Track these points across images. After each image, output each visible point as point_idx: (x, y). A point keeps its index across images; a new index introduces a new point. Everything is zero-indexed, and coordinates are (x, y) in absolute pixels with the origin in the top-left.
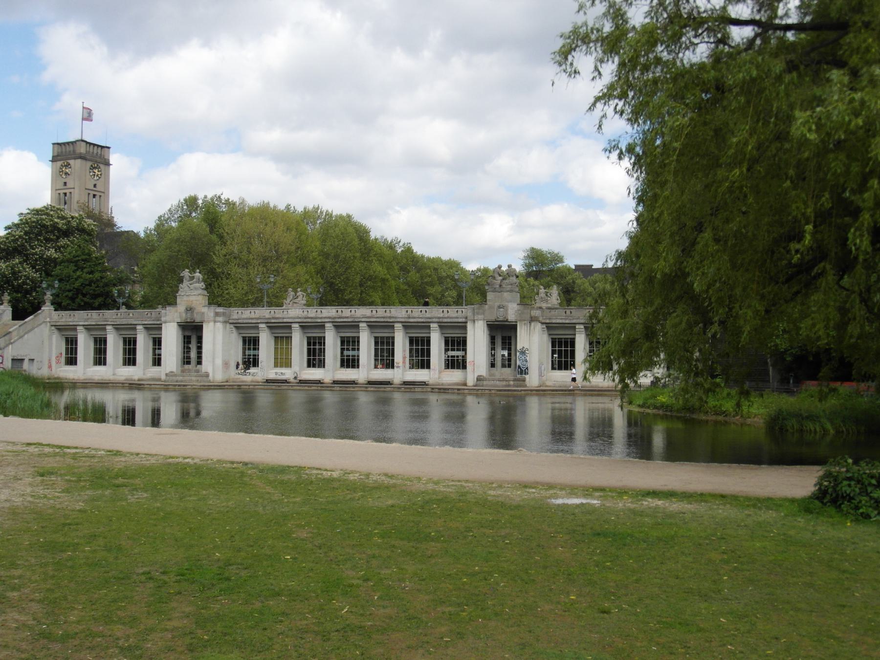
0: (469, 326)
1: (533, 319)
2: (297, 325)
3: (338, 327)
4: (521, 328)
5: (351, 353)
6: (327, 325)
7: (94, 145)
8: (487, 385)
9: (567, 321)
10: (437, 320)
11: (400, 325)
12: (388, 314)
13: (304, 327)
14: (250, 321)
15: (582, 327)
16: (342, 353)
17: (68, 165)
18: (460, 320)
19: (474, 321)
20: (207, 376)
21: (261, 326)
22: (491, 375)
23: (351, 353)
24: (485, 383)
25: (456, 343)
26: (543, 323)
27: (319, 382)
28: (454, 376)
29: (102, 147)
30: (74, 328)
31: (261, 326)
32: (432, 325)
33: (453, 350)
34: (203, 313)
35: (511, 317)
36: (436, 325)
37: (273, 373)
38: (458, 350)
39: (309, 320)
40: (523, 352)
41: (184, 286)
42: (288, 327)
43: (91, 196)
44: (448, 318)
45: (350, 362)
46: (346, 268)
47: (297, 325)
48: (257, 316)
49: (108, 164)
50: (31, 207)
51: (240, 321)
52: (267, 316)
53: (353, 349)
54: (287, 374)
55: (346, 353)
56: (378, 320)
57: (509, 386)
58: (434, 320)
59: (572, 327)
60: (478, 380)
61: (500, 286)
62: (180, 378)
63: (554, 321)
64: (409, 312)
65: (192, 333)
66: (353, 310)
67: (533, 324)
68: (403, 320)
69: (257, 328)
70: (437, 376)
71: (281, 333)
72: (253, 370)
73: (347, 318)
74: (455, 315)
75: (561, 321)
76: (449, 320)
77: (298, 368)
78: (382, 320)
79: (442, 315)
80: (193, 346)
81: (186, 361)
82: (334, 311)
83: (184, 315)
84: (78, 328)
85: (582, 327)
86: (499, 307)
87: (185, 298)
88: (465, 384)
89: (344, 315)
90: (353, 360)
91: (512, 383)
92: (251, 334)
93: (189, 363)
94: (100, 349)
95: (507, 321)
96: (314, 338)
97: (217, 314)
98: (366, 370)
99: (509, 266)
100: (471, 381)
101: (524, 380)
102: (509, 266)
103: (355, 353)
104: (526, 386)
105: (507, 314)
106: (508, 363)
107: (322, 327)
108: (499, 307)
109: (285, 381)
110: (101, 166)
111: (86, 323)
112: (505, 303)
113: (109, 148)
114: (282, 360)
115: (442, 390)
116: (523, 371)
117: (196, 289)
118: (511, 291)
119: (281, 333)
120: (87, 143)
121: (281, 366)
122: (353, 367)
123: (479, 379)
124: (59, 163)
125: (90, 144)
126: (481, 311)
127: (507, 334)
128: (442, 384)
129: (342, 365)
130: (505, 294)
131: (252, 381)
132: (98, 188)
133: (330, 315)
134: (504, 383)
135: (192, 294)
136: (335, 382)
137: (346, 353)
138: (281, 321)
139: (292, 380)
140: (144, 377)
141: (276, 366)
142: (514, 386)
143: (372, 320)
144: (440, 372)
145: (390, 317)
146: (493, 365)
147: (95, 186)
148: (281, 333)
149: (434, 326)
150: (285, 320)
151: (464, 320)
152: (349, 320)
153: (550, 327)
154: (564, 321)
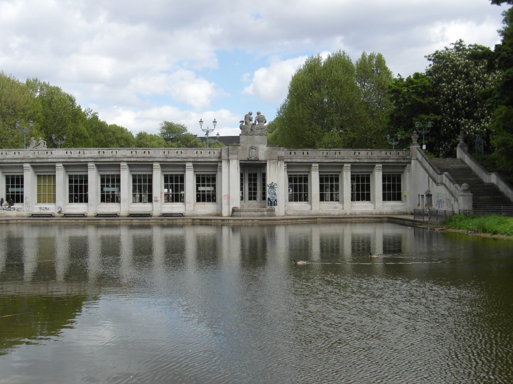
0: (224, 165)
1: (280, 159)
2: (61, 165)
6: (89, 164)
8: (244, 216)
9: (305, 161)
10: (192, 160)
11: (158, 164)
12: (147, 155)
14: (15, 161)
18: (213, 160)
19: (229, 161)
21: (25, 165)
22: (242, 206)
24: (242, 213)
25: (208, 180)
27: (83, 215)
28: (206, 209)
31: (25, 165)
33: (204, 186)
35: (262, 157)
36: (191, 164)
37: (37, 208)
38: (208, 186)
39: (73, 160)
40: (272, 187)
42: (52, 167)
44: (202, 158)
45: (114, 198)
47: (61, 165)
51: (4, 161)
52: (32, 156)
54: (51, 208)
56: (138, 160)
57: (263, 216)
60: (233, 211)
61: (252, 130)
63: (294, 161)
64: (166, 153)
66: (114, 152)
67: (279, 163)
69: (22, 167)
70: (192, 208)
72: (16, 206)
73: (109, 158)
74: (208, 155)
76: (203, 160)
77: (63, 204)
78: (142, 160)
79: (196, 156)
82: (96, 152)
86: (252, 148)
88: (220, 215)
89: (106, 155)
91: (266, 213)
92: (15, 172)
95: (258, 160)
96: (76, 176)
98: (127, 204)
99: (258, 114)
100: (226, 212)
101: (273, 210)
104: (275, 216)
105: (258, 154)
106: (252, 197)
107: (85, 166)
108: (252, 148)
109: (51, 216)
114: (47, 195)
115: (204, 222)
116: (273, 203)
118: (261, 135)
119: (43, 172)
121: (44, 202)
126: (235, 152)
127: (253, 172)
128: (197, 216)
130: (256, 137)
131: (17, 216)
134: (259, 213)
136: (98, 215)
137: (106, 189)
138: (45, 160)
139: (57, 214)
141: (39, 201)
142: (268, 216)
143: (133, 160)
145: (149, 158)
146: (242, 198)
148: (45, 172)
149: (189, 165)
150: (49, 160)
151: (216, 160)
152: (111, 160)
153: (289, 166)
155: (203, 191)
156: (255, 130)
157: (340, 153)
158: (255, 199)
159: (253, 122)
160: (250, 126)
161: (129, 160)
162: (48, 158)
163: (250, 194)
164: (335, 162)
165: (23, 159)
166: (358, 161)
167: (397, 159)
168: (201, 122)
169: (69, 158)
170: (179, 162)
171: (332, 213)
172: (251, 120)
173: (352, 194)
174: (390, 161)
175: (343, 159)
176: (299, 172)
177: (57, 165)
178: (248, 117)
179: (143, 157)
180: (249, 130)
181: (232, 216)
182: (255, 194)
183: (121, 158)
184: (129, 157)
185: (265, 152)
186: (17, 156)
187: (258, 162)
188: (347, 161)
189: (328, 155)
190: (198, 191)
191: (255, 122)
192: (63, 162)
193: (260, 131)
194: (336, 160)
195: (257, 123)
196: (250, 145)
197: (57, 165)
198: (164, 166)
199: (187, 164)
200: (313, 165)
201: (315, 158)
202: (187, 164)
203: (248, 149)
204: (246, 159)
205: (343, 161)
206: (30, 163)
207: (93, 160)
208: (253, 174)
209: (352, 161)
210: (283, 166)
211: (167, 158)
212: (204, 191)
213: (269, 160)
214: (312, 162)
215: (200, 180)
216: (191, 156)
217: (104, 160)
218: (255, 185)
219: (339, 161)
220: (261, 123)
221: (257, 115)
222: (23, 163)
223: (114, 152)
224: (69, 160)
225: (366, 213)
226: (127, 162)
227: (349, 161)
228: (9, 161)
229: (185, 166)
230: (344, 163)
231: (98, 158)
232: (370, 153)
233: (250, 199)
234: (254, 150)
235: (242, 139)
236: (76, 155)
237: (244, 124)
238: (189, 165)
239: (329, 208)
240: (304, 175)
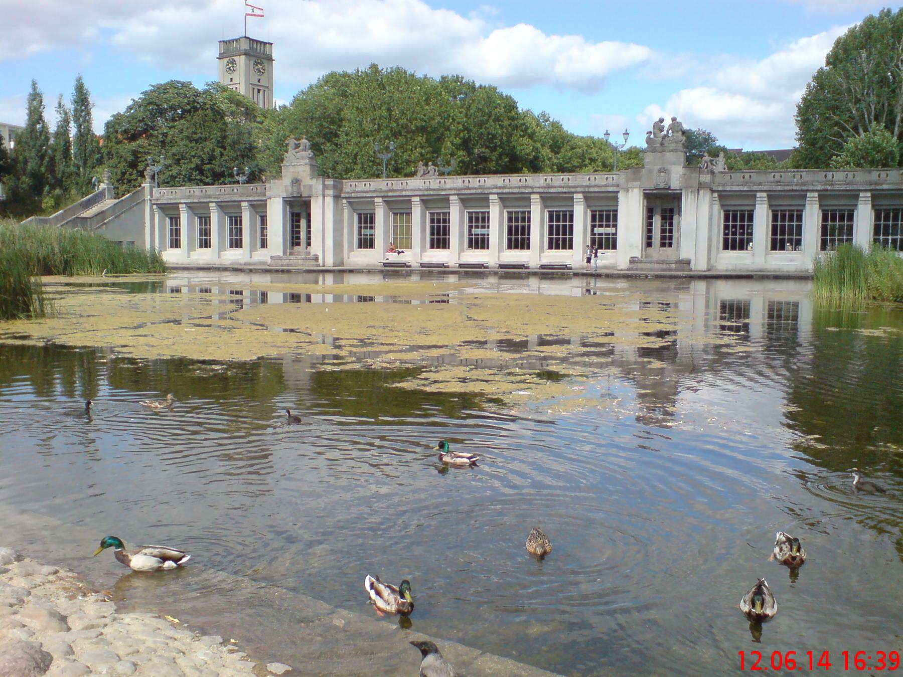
0: (621, 196)
1: (701, 186)
3: (465, 201)
4: (687, 195)
5: (479, 231)
6: (451, 198)
7: (257, 41)
11: (538, 196)
12: (523, 183)
13: (426, 202)
14: (364, 195)
15: (765, 195)
16: (470, 231)
17: (233, 62)
18: (610, 189)
20: (317, 259)
23: (479, 231)
24: (640, 266)
25: (604, 216)
29: (265, 43)
30: (175, 207)
33: (601, 226)
34: (311, 186)
35: (675, 183)
36: (580, 196)
38: (608, 226)
39: (432, 193)
41: (290, 155)
43: (256, 91)
44: (595, 186)
45: (480, 243)
46: (481, 137)
47: (418, 199)
48: (372, 188)
49: (270, 59)
50: (154, 84)
52: (384, 188)
53: (483, 227)
55: (474, 231)
56: (511, 191)
57: (670, 270)
58: (579, 189)
59: (752, 195)
61: (662, 144)
62: (285, 262)
63: (728, 188)
64: (549, 181)
65: (299, 210)
68: (541, 190)
71: (399, 207)
73: (475, 189)
75: (737, 188)
76: (596, 189)
78: (516, 191)
79: (588, 183)
80: (303, 223)
81: (295, 241)
83: (290, 188)
84: (180, 206)
85: (765, 195)
86: (660, 171)
87: (291, 169)
90: (483, 240)
93: (298, 244)
94: (206, 229)
97: (325, 187)
99: (674, 120)
103: (484, 231)
104: (691, 270)
105: (669, 179)
108: (660, 171)
110: (264, 61)
111: (189, 201)
112: (667, 167)
113: (271, 44)
117: (303, 158)
118: (675, 151)
120: (250, 39)
122: (483, 247)
124: (226, 60)
125: (254, 40)
127: (668, 206)
129: (470, 246)
132: (262, 83)
133: (455, 186)
135: (298, 165)
137: (474, 231)
140: (252, 261)
142: (676, 270)
145: (526, 187)
146: (649, 245)
147: (259, 81)
148: (399, 207)
149: (578, 197)
150: (404, 193)
151: (615, 189)
153: (723, 196)
154: (741, 188)
155: (600, 234)
156: (666, 144)
157: (801, 177)
159: (665, 133)
161: (500, 191)
162: (402, 190)
163: (663, 238)
164: (792, 190)
165: (374, 191)
166: (829, 188)
167: (897, 184)
169: (427, 190)
170: (565, 193)
171: (786, 269)
172: (662, 131)
174: (885, 187)
176: (739, 204)
177: (413, 199)
179: (519, 187)
180: (658, 145)
183: (489, 188)
184: (500, 188)
185: (680, 177)
186: (367, 188)
188: (811, 188)
189: (782, 180)
190: (593, 233)
191: (668, 132)
192: (420, 196)
193: (674, 145)
194: (794, 188)
196: (659, 167)
197: (413, 199)
198: (589, 198)
199: (575, 196)
200: (758, 195)
201: (760, 184)
202: (575, 196)
205: (804, 188)
206: (382, 197)
207: (456, 192)
209: (820, 187)
210: (705, 198)
211: (549, 187)
212: (601, 234)
213: (687, 188)
214: (756, 191)
216: (581, 184)
217: (469, 192)
219: (798, 188)
220: (675, 134)
222: (373, 197)
223: (482, 180)
224: (426, 193)
226: (498, 194)
227: (815, 188)
228: (359, 195)
229: (572, 198)
230: (807, 191)
231: (461, 189)
232: (850, 175)
233: (663, 245)
235: (648, 158)
236: (436, 186)
237: (652, 136)
238: (578, 197)
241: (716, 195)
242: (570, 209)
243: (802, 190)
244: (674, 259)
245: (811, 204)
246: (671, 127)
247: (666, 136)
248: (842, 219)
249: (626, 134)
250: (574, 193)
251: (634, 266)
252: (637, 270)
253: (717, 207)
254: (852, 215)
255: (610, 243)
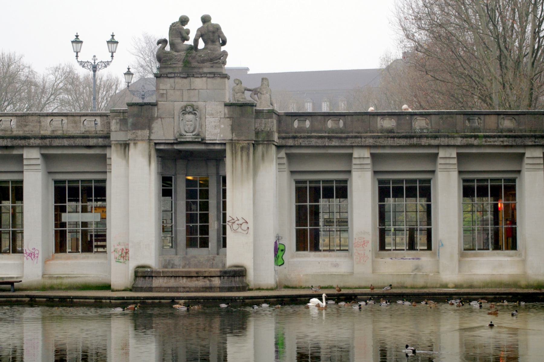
8: (159, 289)
24: (157, 282)
25: (80, 193)
26: (279, 147)
32: (27, 154)
57: (210, 289)
86: (184, 111)
95: (202, 142)
99: (206, 20)
102: (206, 20)
104: (245, 288)
108: (184, 111)
123: (142, 273)
142: (222, 289)
144: (46, 260)
158: (205, 244)
159: (190, 42)
160: (183, 54)
163: (190, 231)
168: (77, 41)
173: (467, 231)
175: (436, 137)
178: (178, 30)
181: (133, 289)
182: (205, 230)
187: (203, 147)
191: (196, 41)
195: (201, 45)
203: (176, 113)
204: (170, 137)
208: (192, 179)
215: (64, 194)
218: (205, 206)
220: (210, 46)
221: (201, 24)
225: (500, 284)
227: (452, 142)
233: (191, 243)
234: (190, 117)
237: (168, 48)
239: (399, 268)
240: (338, 181)
241: (283, 154)
242: (15, 177)
243: (430, 146)
244: (216, 270)
245: (447, 170)
246: (201, 34)
247: (195, 47)
248: (496, 195)
249: (112, 42)
250: (23, 147)
251: (141, 283)
252: (150, 289)
253: (286, 175)
254: (513, 188)
255: (92, 241)
